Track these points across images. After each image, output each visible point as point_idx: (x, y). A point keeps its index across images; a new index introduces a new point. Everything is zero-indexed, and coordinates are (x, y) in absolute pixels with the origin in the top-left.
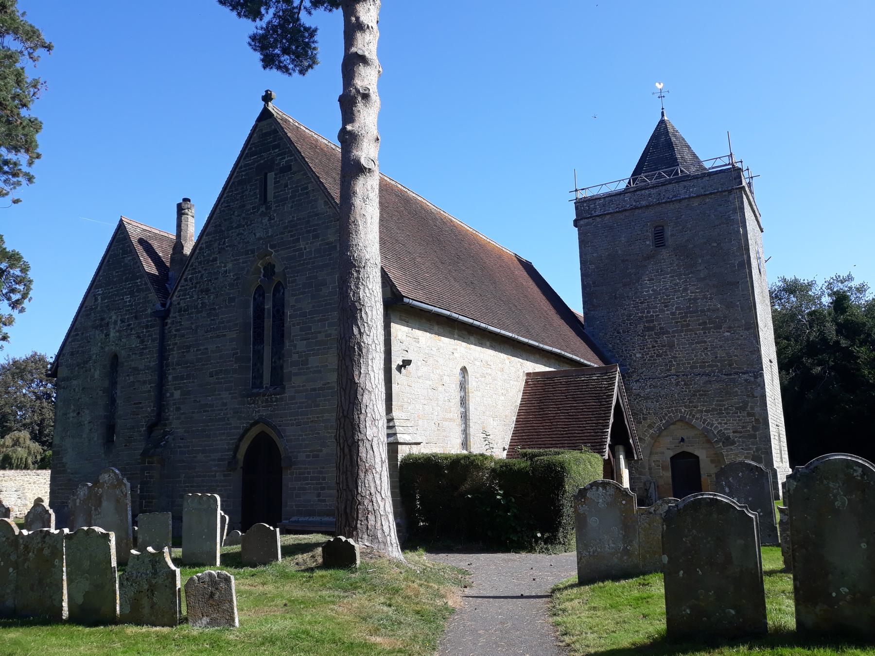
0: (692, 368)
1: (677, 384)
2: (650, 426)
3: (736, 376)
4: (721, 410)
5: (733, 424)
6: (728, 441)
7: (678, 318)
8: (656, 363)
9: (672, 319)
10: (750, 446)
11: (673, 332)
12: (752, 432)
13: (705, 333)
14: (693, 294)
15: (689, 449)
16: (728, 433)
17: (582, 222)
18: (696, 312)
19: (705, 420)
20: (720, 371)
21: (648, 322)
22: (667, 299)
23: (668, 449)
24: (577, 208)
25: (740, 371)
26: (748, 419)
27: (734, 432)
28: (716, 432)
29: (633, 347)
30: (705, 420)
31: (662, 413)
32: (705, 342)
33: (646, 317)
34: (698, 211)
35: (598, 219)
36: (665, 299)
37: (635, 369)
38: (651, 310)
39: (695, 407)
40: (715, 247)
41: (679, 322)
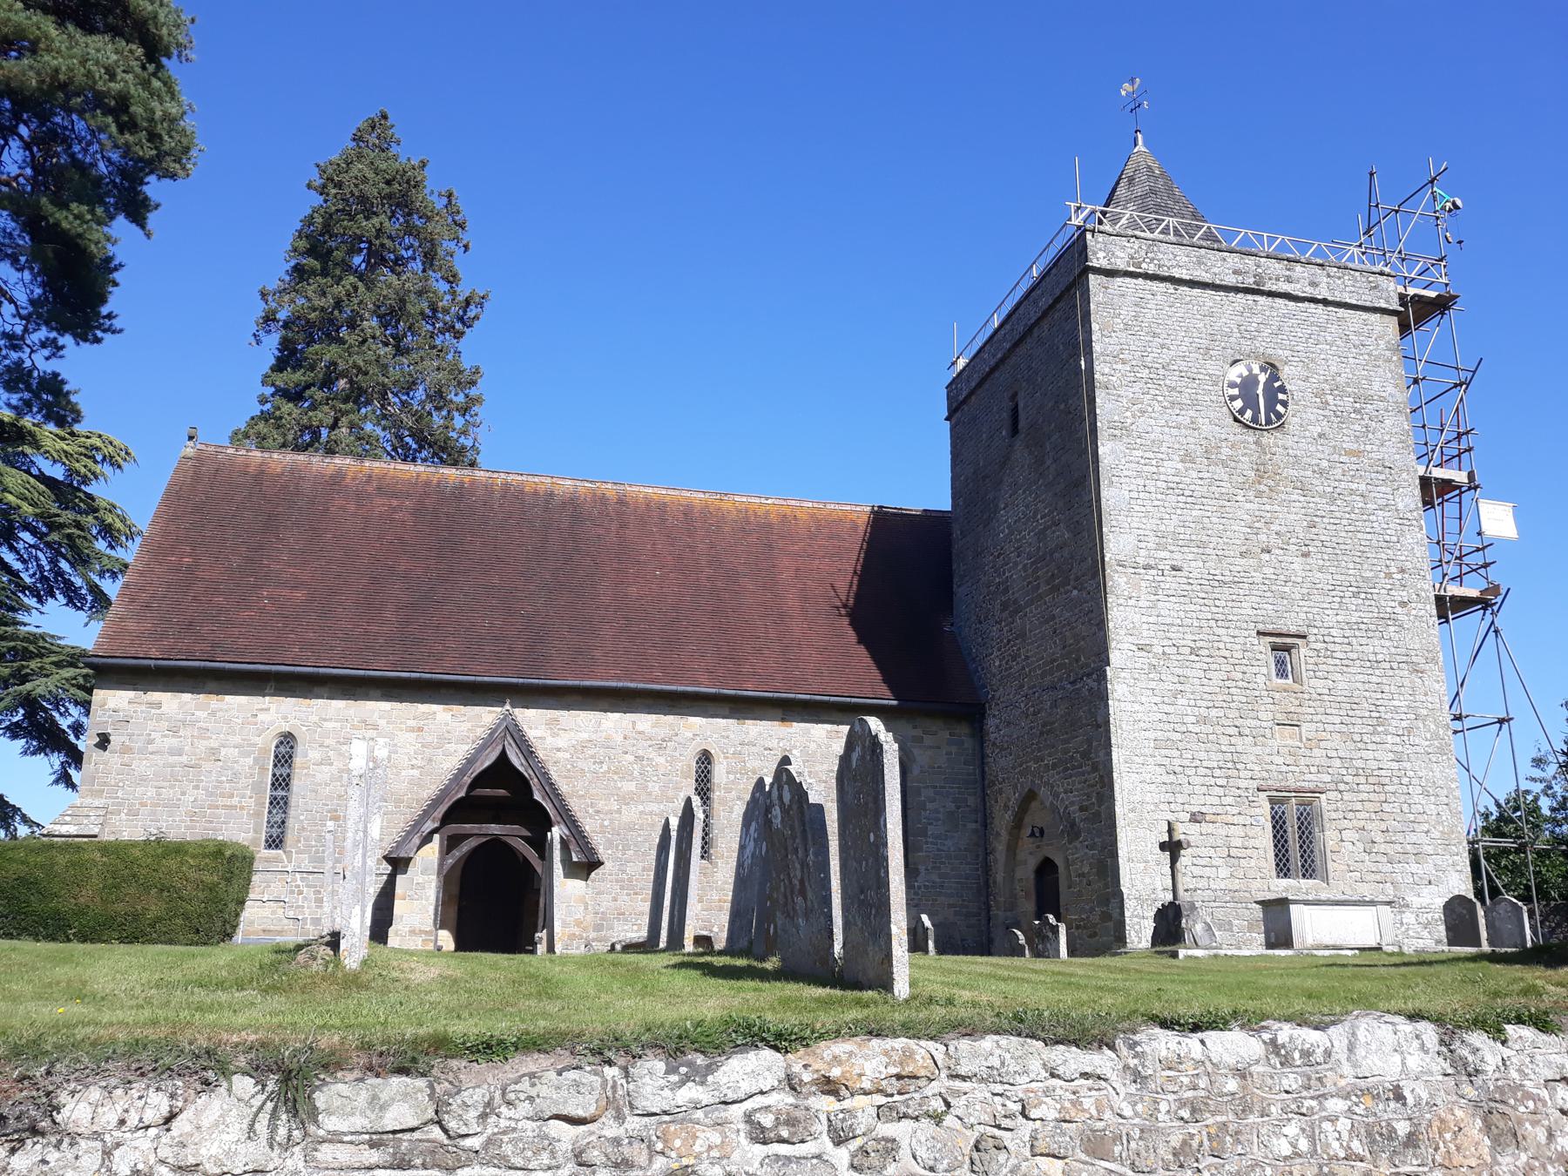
2: (1006, 807)
30: (1052, 787)
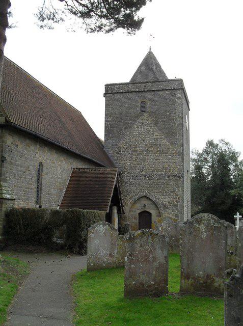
2: (131, 198)
6: (165, 207)
15: (148, 210)
17: (107, 95)
18: (156, 145)
20: (165, 174)
35: (115, 95)
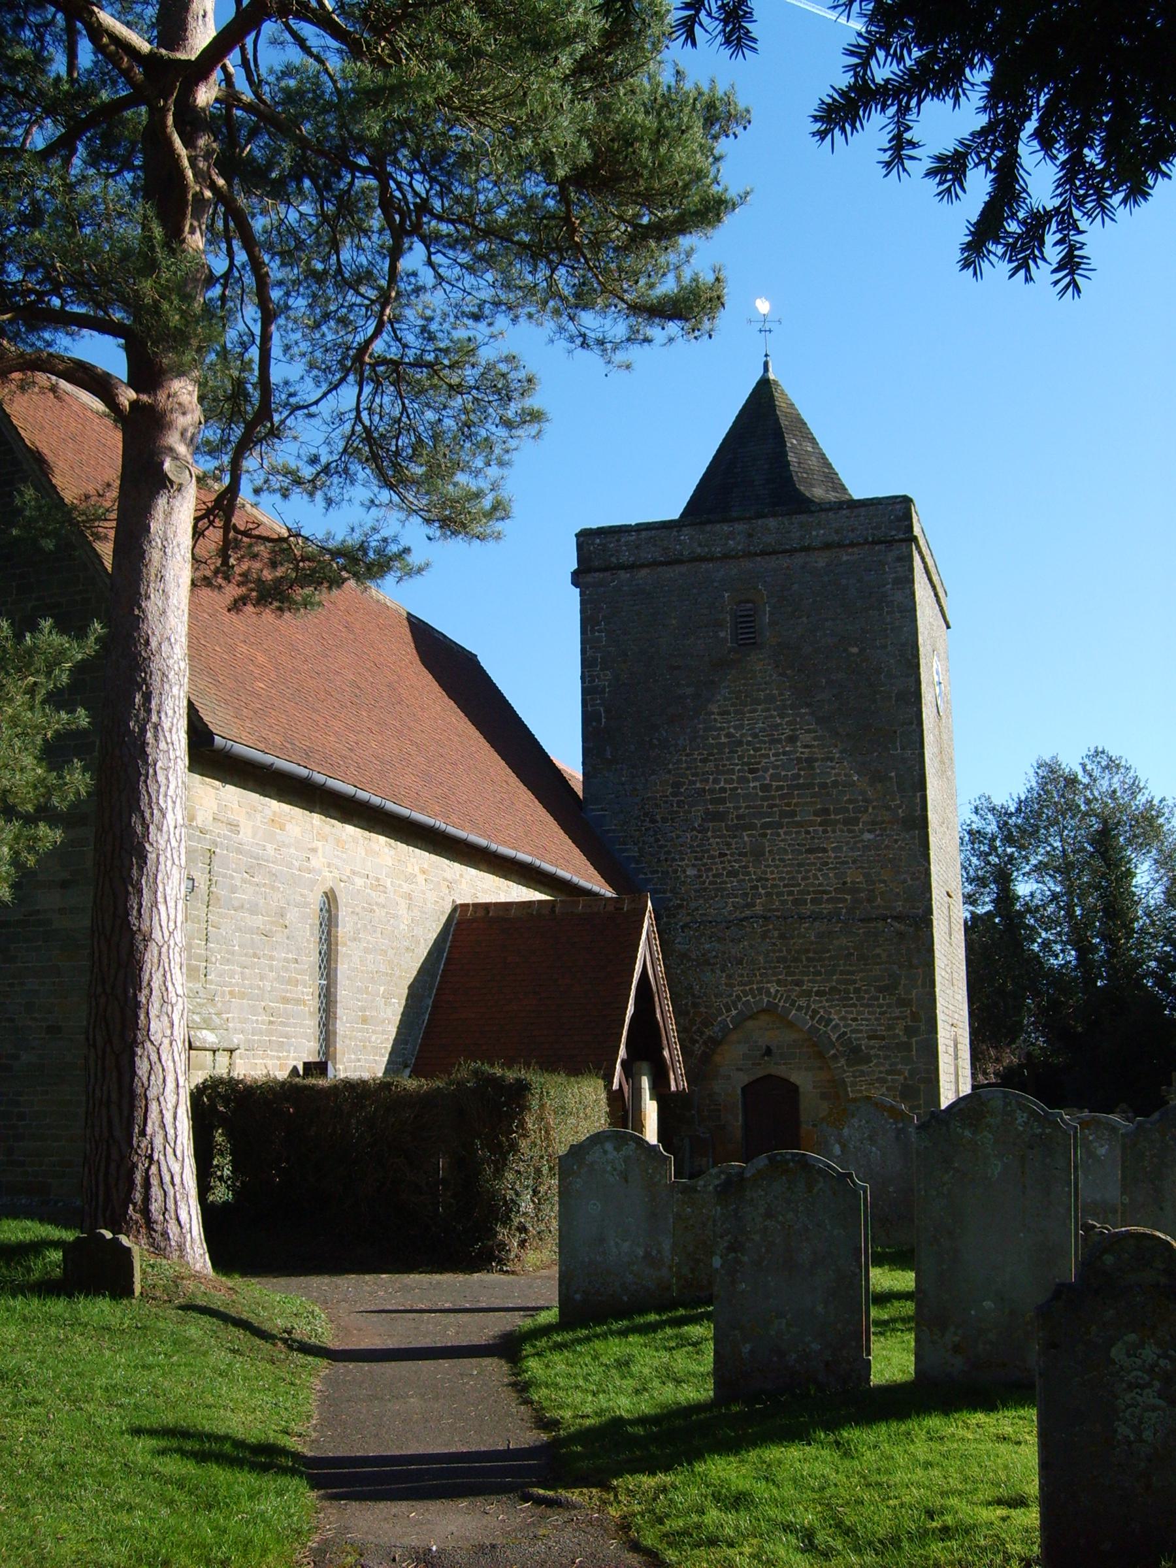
0: (796, 902)
1: (765, 935)
3: (880, 924)
4: (847, 991)
5: (866, 1020)
6: (856, 1055)
7: (773, 797)
8: (725, 889)
9: (763, 799)
10: (899, 1066)
11: (765, 826)
12: (905, 1039)
13: (825, 832)
14: (806, 750)
15: (781, 1070)
16: (858, 1039)
17: (589, 578)
18: (810, 786)
19: (815, 1012)
21: (712, 801)
22: (755, 757)
23: (738, 1069)
24: (580, 547)
25: (888, 913)
26: (897, 1012)
27: (870, 1038)
28: (834, 1038)
29: (681, 853)
30: (815, 1012)
31: (731, 995)
32: (825, 850)
33: (712, 791)
34: (826, 579)
35: (624, 575)
36: (750, 756)
37: (682, 899)
38: (722, 778)
39: (797, 985)
40: (854, 655)
41: (775, 806)
